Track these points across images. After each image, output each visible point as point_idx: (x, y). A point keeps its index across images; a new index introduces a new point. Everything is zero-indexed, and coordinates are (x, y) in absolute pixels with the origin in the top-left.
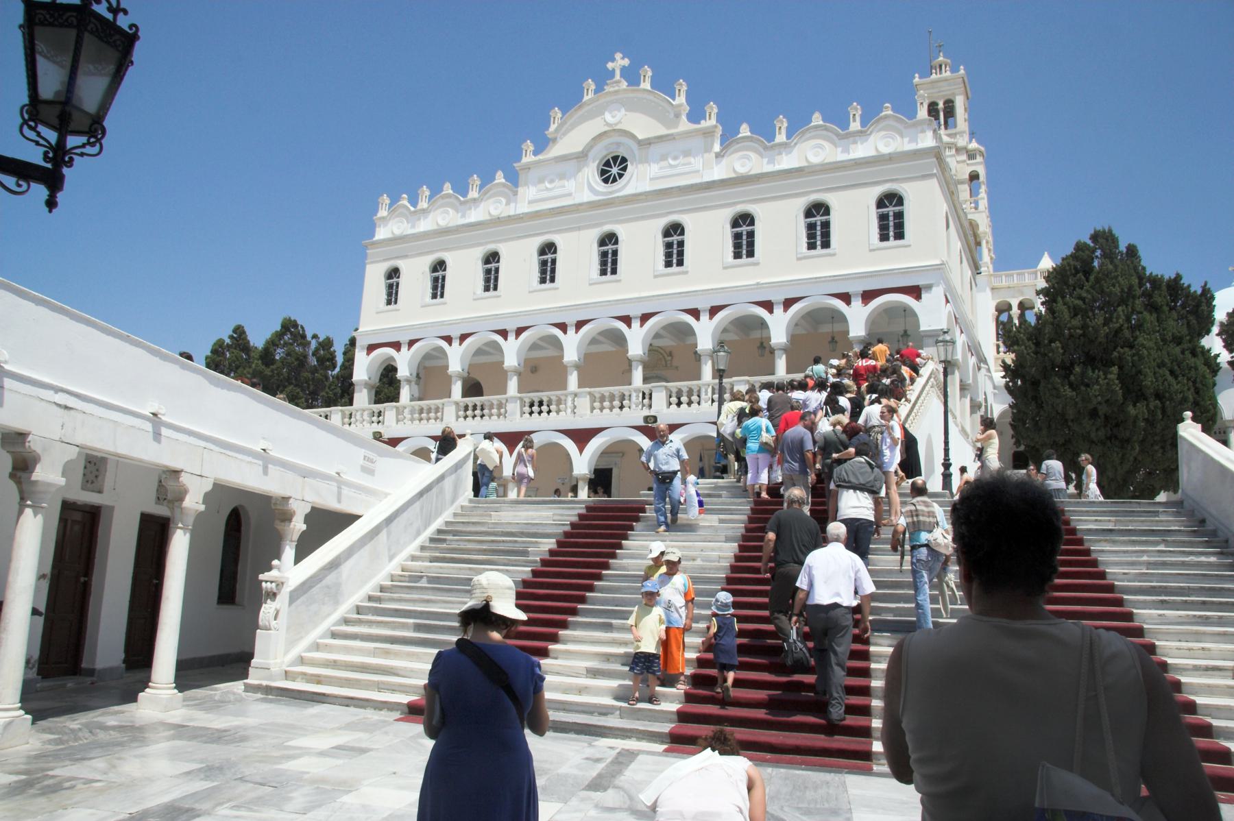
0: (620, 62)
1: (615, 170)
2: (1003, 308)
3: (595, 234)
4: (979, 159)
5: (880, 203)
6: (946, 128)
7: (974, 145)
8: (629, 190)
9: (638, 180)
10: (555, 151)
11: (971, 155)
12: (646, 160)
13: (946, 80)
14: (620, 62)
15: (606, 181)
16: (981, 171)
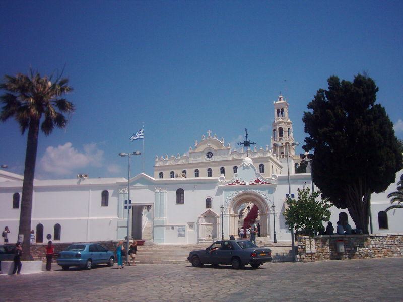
0: (209, 132)
1: (210, 155)
2: (296, 164)
3: (206, 168)
4: (290, 125)
5: (260, 166)
6: (282, 116)
7: (289, 121)
8: (213, 160)
9: (215, 158)
10: (197, 150)
11: (288, 124)
12: (216, 155)
13: (282, 103)
14: (209, 132)
15: (208, 157)
16: (291, 128)
